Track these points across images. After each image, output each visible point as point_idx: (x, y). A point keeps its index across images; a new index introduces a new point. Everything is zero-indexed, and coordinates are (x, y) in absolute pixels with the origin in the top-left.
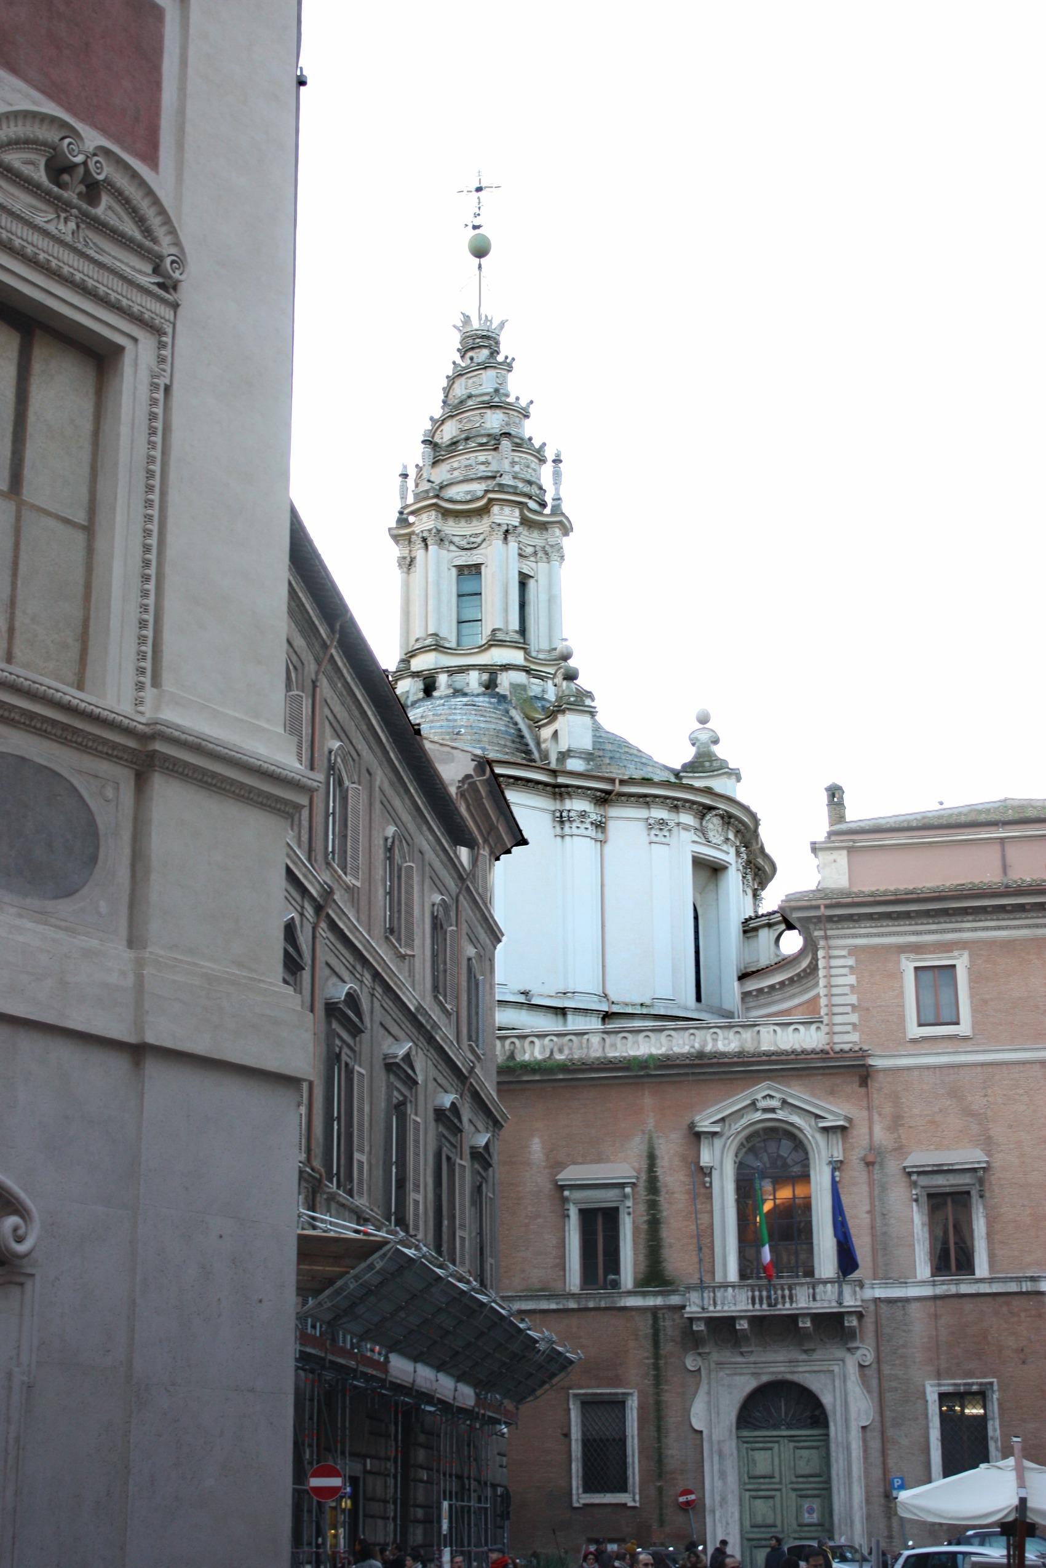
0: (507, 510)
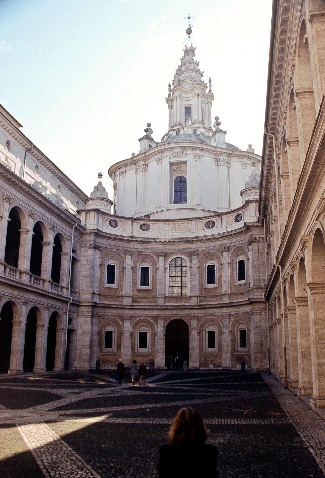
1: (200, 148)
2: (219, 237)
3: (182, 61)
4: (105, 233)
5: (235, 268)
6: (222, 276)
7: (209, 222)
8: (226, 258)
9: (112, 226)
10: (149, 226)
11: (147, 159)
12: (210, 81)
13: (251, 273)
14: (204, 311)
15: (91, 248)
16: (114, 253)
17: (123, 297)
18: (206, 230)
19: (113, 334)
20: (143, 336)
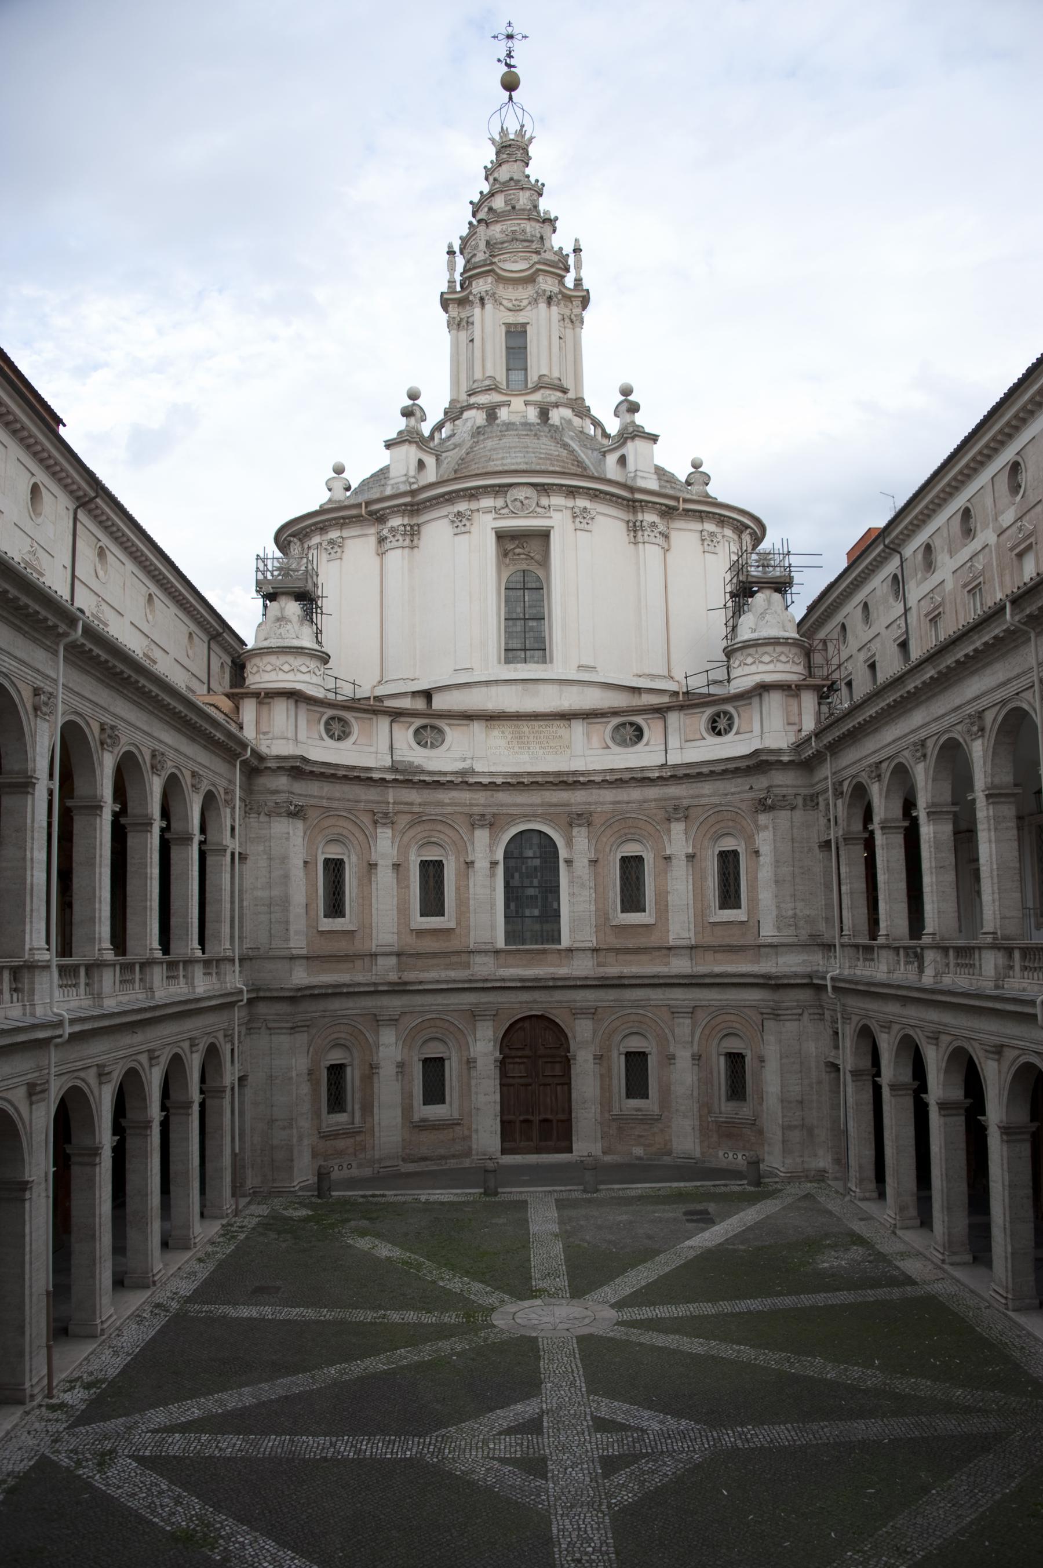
0: (550, 280)
1: (589, 489)
2: (658, 777)
3: (489, 173)
4: (316, 762)
5: (710, 872)
6: (668, 892)
7: (623, 725)
8: (678, 840)
9: (331, 737)
10: (440, 731)
11: (418, 510)
12: (577, 250)
13: (766, 896)
14: (612, 995)
15: (279, 815)
16: (342, 822)
17: (374, 956)
18: (616, 749)
19: (349, 1070)
20: (434, 1068)
